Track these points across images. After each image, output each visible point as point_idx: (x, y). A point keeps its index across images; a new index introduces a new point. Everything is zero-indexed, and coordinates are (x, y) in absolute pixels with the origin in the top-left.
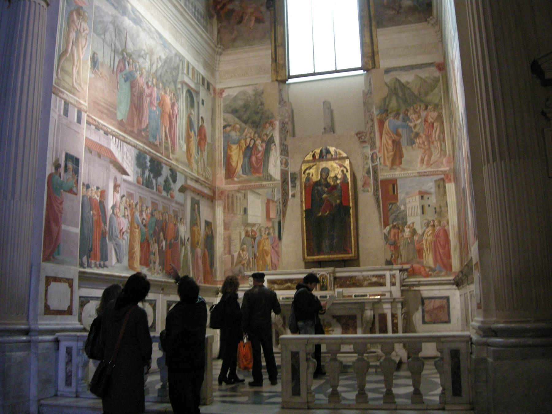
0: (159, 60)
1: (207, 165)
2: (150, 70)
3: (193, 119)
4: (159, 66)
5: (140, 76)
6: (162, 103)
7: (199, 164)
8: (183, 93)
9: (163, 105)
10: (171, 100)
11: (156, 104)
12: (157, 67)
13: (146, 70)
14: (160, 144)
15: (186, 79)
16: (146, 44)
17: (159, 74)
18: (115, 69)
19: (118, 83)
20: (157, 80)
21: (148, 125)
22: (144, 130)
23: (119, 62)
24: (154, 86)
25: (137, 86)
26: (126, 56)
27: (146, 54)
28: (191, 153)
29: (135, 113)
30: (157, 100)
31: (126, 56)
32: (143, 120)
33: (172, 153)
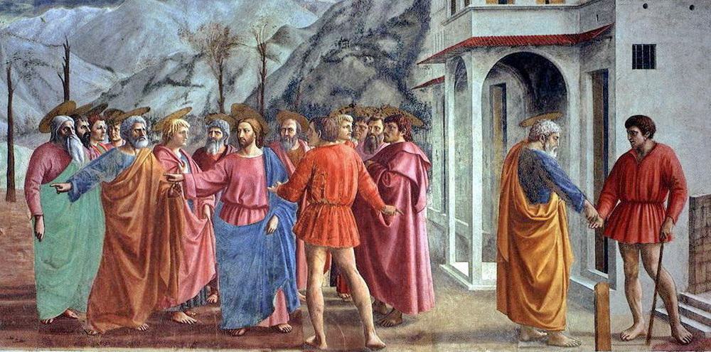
0: (274, 48)
1: (693, 285)
2: (221, 102)
3: (553, 155)
4: (272, 66)
5: (156, 152)
6: (304, 179)
7: (617, 301)
8: (461, 84)
9: (309, 187)
10: (369, 144)
11: (260, 199)
12: (263, 74)
13: (190, 118)
14: (296, 319)
15: (482, 26)
16: (184, 32)
17: (276, 91)
18: (20, 185)
19: (36, 218)
20: (264, 116)
21: (213, 283)
22: (186, 307)
23: (34, 159)
24: (243, 146)
25: (142, 188)
26: (70, 123)
27: (190, 68)
28: (540, 278)
29: (134, 272)
30: (269, 180)
31: (70, 123)
32: (182, 275)
33: (382, 319)
